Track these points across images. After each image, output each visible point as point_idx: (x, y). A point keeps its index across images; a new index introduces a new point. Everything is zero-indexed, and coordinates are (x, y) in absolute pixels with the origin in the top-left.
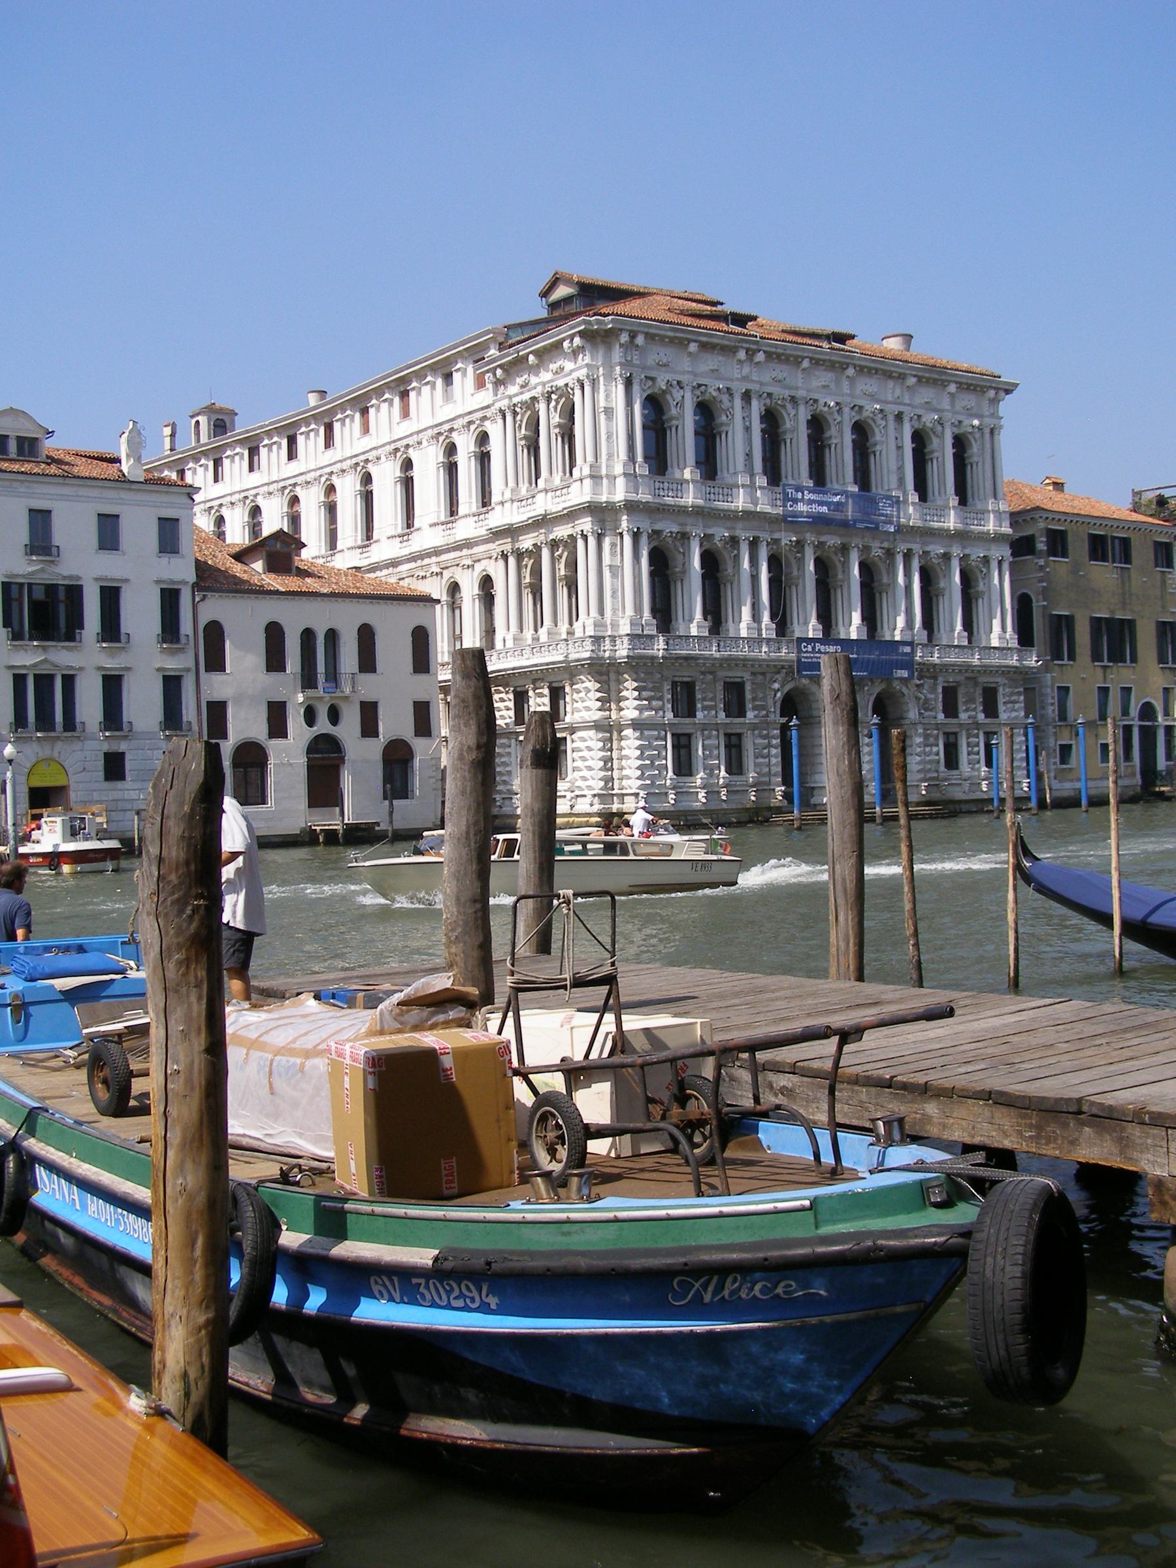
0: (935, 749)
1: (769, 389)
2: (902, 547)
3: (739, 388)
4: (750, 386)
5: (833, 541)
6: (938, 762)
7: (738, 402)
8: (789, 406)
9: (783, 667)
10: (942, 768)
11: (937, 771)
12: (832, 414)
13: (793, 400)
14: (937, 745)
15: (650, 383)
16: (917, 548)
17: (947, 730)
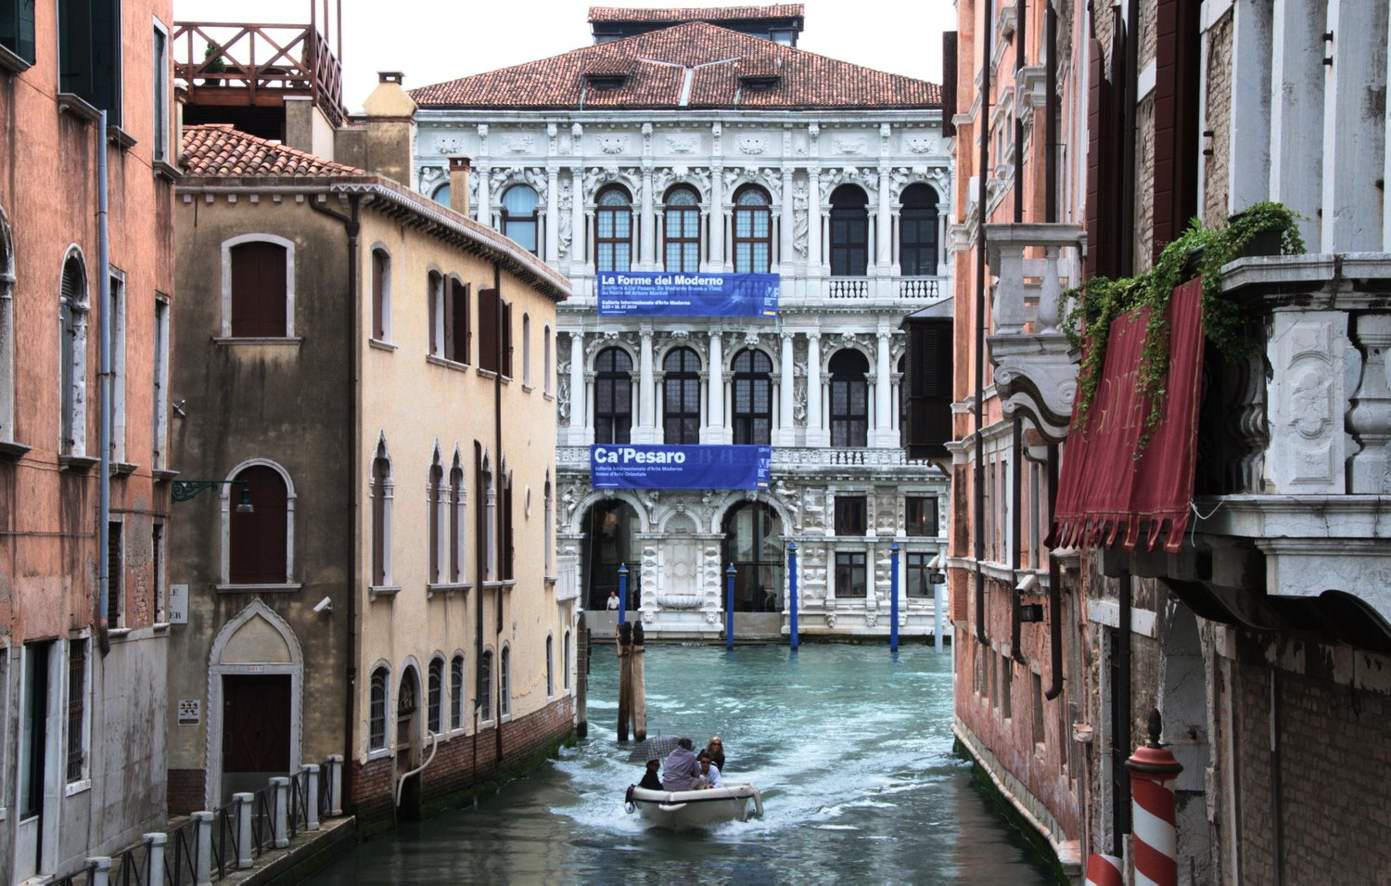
0: (822, 571)
1: (600, 164)
2: (789, 330)
3: (553, 167)
4: (565, 164)
5: (680, 330)
6: (825, 587)
7: (553, 182)
8: (634, 179)
9: (574, 477)
10: (831, 595)
11: (824, 598)
12: (701, 180)
13: (637, 170)
14: (825, 567)
15: (437, 173)
16: (813, 330)
17: (839, 549)
